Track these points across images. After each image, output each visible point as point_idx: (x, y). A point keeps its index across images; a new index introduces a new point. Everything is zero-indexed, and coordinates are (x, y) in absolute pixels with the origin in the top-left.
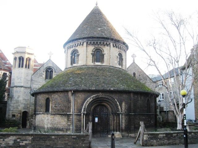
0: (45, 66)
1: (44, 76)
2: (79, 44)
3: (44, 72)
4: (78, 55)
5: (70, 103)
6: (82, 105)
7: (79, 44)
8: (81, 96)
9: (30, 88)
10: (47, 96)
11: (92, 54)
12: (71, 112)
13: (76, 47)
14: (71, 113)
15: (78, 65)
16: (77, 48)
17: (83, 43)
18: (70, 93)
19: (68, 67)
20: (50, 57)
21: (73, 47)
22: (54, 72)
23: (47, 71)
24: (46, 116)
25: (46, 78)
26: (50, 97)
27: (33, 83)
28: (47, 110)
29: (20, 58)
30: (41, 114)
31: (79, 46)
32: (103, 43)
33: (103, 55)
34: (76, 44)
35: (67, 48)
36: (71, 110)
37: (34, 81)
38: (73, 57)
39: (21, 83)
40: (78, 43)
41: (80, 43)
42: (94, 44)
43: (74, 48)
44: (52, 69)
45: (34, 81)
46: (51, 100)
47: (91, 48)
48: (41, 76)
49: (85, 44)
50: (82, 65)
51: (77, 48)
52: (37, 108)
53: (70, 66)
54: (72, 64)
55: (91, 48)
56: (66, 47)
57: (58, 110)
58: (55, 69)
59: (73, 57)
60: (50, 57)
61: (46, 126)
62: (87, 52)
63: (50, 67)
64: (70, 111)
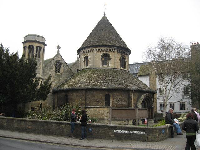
0: (55, 60)
1: (54, 69)
2: (111, 50)
3: (54, 65)
4: (110, 59)
5: (131, 99)
6: (137, 101)
7: (111, 50)
8: (137, 94)
9: (43, 80)
10: (106, 93)
11: (120, 60)
12: (132, 106)
13: (108, 52)
14: (132, 107)
15: (110, 67)
16: (108, 53)
17: (115, 50)
18: (131, 92)
19: (97, 67)
20: (59, 51)
21: (103, 51)
22: (62, 66)
23: (56, 65)
24: (105, 109)
25: (56, 71)
26: (110, 93)
27: (45, 75)
28: (108, 104)
29: (37, 47)
30: (98, 107)
31: (110, 52)
32: (126, 53)
33: (125, 62)
34: (107, 49)
35: (95, 50)
36: (132, 105)
37: (46, 73)
38: (103, 59)
39: (39, 74)
40: (110, 49)
41: (112, 50)
42: (121, 53)
43: (105, 52)
44: (61, 63)
45: (46, 73)
46: (111, 95)
47: (119, 55)
48: (52, 69)
49: (116, 51)
50: (114, 68)
51: (108, 53)
52: (88, 102)
53: (101, 67)
54: (102, 64)
55: (119, 55)
56: (95, 49)
57: (120, 105)
58: (63, 63)
59: (103, 59)
60: (59, 51)
61: (106, 118)
62: (117, 57)
63: (59, 61)
64: (131, 106)
